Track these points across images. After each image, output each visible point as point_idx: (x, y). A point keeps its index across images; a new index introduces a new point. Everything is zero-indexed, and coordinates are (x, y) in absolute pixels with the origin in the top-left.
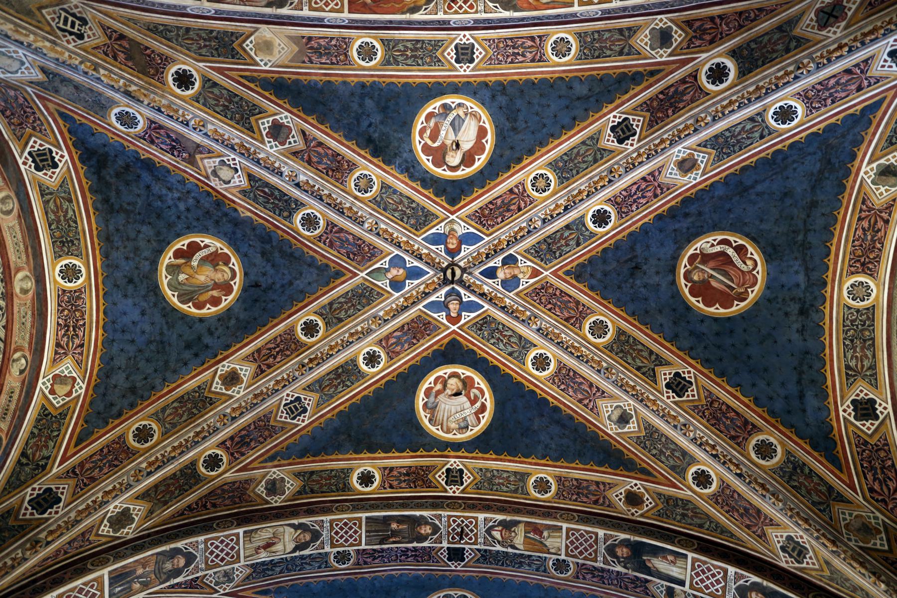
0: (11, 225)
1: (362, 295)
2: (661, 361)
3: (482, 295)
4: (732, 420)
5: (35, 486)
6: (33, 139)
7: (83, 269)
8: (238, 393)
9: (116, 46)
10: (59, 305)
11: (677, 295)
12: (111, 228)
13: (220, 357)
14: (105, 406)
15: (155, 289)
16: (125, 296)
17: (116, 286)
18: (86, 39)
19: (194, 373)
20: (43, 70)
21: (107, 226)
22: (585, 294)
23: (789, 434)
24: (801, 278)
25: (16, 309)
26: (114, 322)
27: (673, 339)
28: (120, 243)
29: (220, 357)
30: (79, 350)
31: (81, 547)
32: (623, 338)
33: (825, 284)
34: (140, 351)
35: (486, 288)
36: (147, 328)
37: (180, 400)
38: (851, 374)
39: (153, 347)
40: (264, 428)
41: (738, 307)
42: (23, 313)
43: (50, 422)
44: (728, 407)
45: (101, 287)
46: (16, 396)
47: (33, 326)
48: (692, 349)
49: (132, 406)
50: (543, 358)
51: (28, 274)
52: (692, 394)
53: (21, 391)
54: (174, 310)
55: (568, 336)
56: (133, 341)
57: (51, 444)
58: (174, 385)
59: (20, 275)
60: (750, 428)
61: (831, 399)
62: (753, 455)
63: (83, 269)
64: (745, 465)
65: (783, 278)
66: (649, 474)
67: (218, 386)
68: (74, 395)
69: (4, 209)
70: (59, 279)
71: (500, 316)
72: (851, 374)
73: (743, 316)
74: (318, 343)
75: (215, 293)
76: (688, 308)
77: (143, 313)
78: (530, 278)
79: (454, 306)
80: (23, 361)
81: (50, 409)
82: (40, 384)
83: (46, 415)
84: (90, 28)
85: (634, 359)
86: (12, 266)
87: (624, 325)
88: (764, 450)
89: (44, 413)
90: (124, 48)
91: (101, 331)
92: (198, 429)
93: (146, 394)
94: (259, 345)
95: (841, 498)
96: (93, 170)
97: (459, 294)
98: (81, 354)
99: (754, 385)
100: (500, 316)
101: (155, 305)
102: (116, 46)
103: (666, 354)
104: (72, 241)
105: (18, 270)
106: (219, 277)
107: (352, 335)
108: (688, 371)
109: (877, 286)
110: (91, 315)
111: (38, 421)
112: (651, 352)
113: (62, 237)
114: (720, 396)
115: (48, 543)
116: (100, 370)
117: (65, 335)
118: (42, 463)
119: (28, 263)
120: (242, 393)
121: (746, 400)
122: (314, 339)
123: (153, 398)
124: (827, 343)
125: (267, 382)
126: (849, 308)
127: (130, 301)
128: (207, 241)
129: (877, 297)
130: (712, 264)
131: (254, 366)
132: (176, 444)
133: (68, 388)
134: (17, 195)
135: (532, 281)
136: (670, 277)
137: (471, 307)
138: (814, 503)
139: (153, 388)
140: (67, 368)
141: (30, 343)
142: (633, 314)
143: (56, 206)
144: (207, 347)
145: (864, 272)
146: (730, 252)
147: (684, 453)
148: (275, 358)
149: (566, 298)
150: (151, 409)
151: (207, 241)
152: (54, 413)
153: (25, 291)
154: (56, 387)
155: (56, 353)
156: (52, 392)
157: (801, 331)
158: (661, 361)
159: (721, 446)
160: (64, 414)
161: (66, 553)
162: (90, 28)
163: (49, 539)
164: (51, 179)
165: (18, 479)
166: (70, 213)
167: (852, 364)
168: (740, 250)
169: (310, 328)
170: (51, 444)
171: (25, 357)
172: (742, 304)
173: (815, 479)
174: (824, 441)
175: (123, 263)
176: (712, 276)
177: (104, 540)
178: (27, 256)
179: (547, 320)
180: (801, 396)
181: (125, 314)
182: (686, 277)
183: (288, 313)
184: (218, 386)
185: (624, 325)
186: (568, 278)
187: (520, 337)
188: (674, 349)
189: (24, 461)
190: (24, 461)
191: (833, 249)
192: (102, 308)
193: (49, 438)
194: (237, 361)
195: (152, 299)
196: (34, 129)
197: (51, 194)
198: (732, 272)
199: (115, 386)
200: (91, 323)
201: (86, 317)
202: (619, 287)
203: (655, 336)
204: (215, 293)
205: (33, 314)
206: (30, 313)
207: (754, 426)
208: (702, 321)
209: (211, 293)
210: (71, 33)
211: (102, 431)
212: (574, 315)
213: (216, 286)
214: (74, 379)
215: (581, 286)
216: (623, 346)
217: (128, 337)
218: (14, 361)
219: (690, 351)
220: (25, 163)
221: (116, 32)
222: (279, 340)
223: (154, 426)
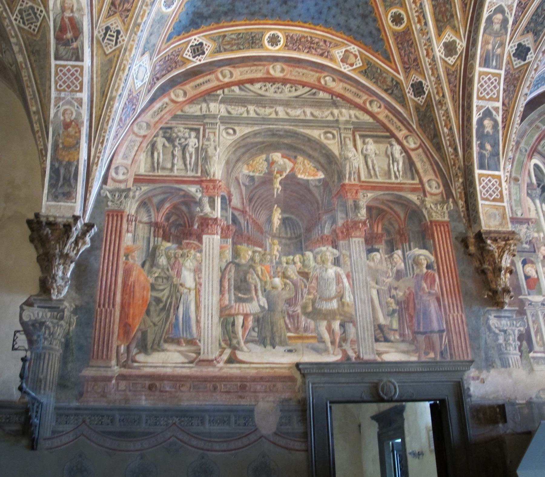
0: (239, 73)
5: (407, 91)
6: (184, 55)
7: (272, 32)
9: (120, 9)
10: (295, 50)
12: (245, 11)
16: (295, 7)
17: (287, 12)
18: (119, 28)
20: (143, 54)
21: (244, 14)
25: (293, 78)
28: (257, 7)
30: (328, 44)
31: (456, 77)
42: (296, 74)
46: (348, 87)
47: (306, 69)
49: (375, 20)
51: (271, 66)
53: (346, 83)
56: (329, 8)
57: (384, 75)
59: (272, 72)
63: (272, 32)
68: (357, 53)
69: (229, 76)
70: (277, 48)
80: (327, 78)
81: (363, 69)
82: (346, 71)
83: (366, 72)
84: (112, 25)
86: (265, 76)
89: (365, 73)
90: (120, 3)
93: (369, 8)
96: (204, 21)
102: (120, 9)
104: (252, 37)
105: (268, 72)
110: (305, 32)
111: (367, 77)
113: (249, 43)
115: (444, 96)
116: (344, 33)
117: (315, 50)
119: (264, 65)
123: (374, 4)
134: (220, 67)
140: (338, 53)
141: (317, 72)
143: (228, 44)
152: (366, 67)
153: (283, 70)
155: (327, 57)
156: (352, 65)
160: (368, 62)
161: (455, 86)
162: (112, 25)
163: (441, 95)
164: (209, 46)
165: (400, 98)
166: (233, 36)
170: (384, 75)
171: (325, 77)
175: (271, 6)
177: (459, 62)
178: (260, 65)
189: (390, 91)
190: (390, 91)
193: (381, 74)
196: (178, 55)
197: (220, 47)
199: (358, 27)
201: (306, 35)
205: (298, 67)
206: (297, 69)
210: (117, 38)
211: (386, 44)
214: (346, 51)
217: (325, 10)
218: (326, 84)
220: (200, 60)
221: (110, 8)
223: (394, 10)
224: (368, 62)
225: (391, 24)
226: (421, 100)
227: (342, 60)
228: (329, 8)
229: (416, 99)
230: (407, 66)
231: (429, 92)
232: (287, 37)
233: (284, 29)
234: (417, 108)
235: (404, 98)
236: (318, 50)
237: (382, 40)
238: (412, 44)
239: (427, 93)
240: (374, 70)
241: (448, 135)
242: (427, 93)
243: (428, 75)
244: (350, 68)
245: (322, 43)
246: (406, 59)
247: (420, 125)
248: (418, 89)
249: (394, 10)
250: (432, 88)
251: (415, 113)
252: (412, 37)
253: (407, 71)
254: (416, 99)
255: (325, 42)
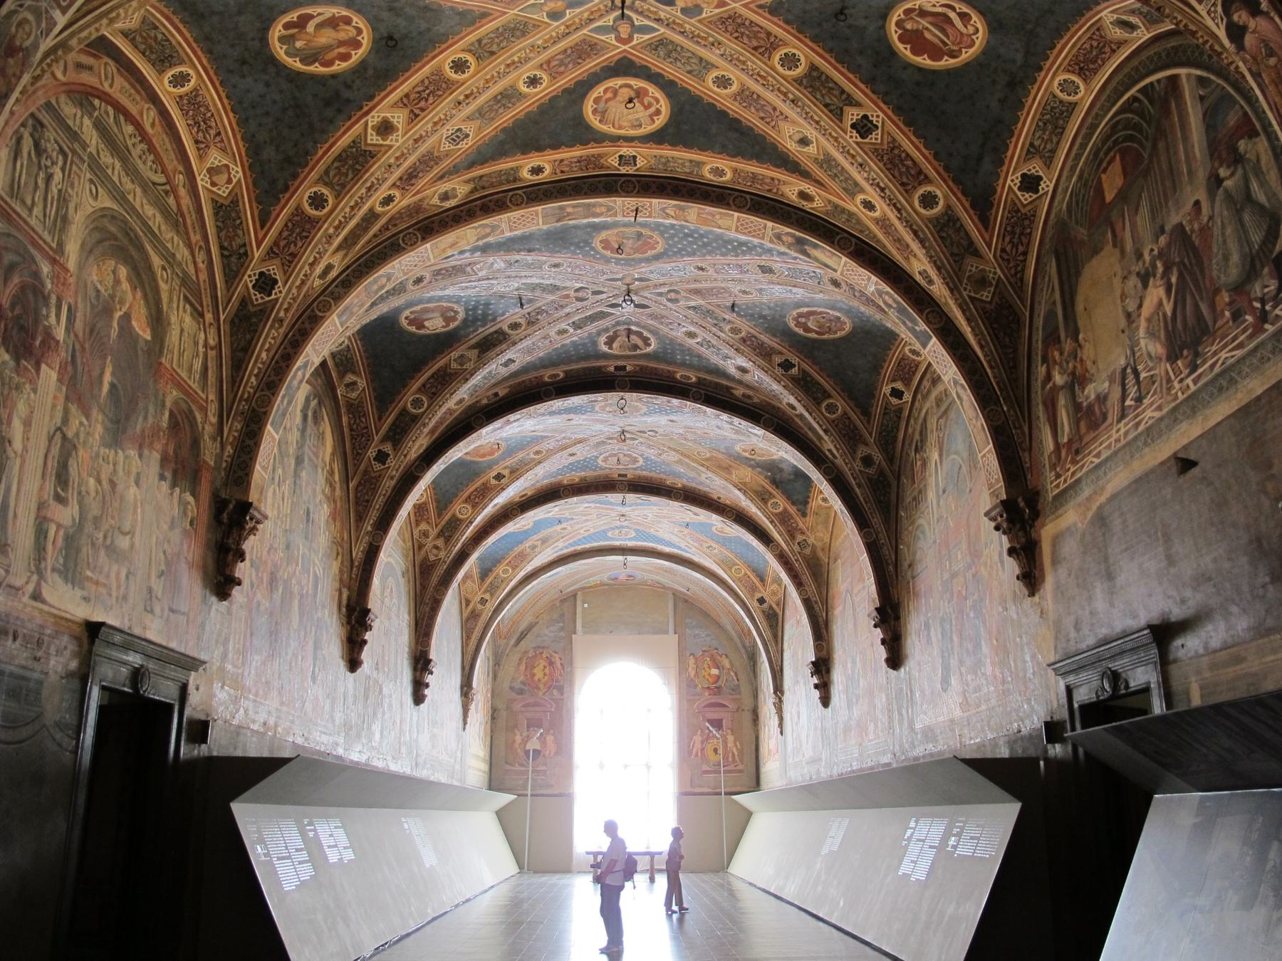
1: (514, 30)
2: (851, 101)
3: (658, 20)
4: (908, 168)
5: (249, 272)
7: (191, 72)
8: (397, 141)
11: (883, 39)
13: (366, 109)
14: (271, 180)
15: (273, 60)
16: (244, 77)
17: (231, 72)
19: (343, 129)
22: (779, 26)
23: (955, 189)
24: (1019, 57)
26: (240, 103)
27: (870, 81)
29: (366, 109)
30: (218, 139)
32: (815, 74)
33: (1040, 69)
34: (278, 120)
35: (662, 15)
36: (277, 97)
37: (339, 158)
38: (1032, 151)
39: (290, 113)
40: (429, 160)
41: (947, 62)
43: (227, 212)
44: (908, 155)
45: (215, 78)
48: (886, 94)
50: (726, 78)
52: (876, 137)
54: (299, 73)
55: (755, 63)
56: (267, 114)
58: (327, 145)
60: (921, 177)
61: (1005, 168)
62: (916, 203)
63: (191, 72)
64: (906, 211)
65: (1002, 51)
66: (822, 185)
67: (372, 138)
68: (235, 181)
70: (172, 89)
71: (678, 39)
72: (1032, 151)
73: (949, 72)
74: (471, 79)
75: (342, 50)
76: (893, 53)
77: (267, 85)
78: (717, 7)
79: (624, 30)
82: (200, 183)
85: (823, 96)
87: (818, 61)
88: (929, 201)
89: (218, 207)
91: (231, 115)
92: (368, 184)
94: (406, 91)
95: (976, 253)
97: (630, 19)
98: (222, 141)
99: (938, 140)
100: (678, 39)
101: (278, 74)
103: (858, 95)
106: (342, 36)
107: (508, 66)
108: (877, 115)
109: (1086, 90)
110: (215, 105)
111: (216, 214)
112: (843, 92)
114: (903, 144)
118: (242, 251)
120: (401, 141)
121: (926, 152)
122: (466, 75)
124: (1022, 118)
125: (423, 126)
126: (1055, 96)
127: (249, 80)
128: (320, 10)
129: (1082, 98)
130: (930, 19)
131: (406, 111)
132: (352, 203)
133: (226, 176)
135: (717, 11)
136: (880, 23)
137: (643, 30)
138: (952, 254)
139: (307, 153)
142: (830, 51)
144: (348, 101)
145: (1079, 75)
146: (952, 15)
147: (856, 184)
148: (427, 100)
149: (756, 29)
150: (314, 175)
151: (320, 10)
152: (226, 203)
154: (215, 179)
155: (199, 149)
156: (214, 184)
157: (1002, 101)
158: (851, 101)
159: (890, 190)
160: (235, 201)
166: (160, 36)
167: (1037, 143)
168: (964, 17)
169: (459, 66)
170: (240, 232)
172: (952, 61)
173: (962, 234)
174: (982, 204)
176: (927, 29)
179: (732, 46)
180: (980, 159)
181: (248, 91)
182: (899, 24)
183: (431, 55)
184: (372, 138)
185: (818, 61)
186: (760, 11)
187: (701, 59)
188: (868, 91)
189: (226, 253)
191: (1059, 46)
192: (223, 95)
193: (236, 227)
194: (387, 108)
195: (272, 70)
198: (950, 31)
200: (218, 110)
201: (211, 108)
202: (819, 25)
203: (851, 76)
204: (342, 50)
207: (926, 177)
208: (905, 68)
209: (337, 51)
212: (765, 46)
213: (341, 43)
214: (227, 166)
215: (775, 19)
216: (814, 81)
219: (885, 97)
222: (426, 82)
223: (325, 191)
224: (235, 201)
225: (306, 197)
226: (258, 298)
227: (210, 171)
228: (267, 114)
229: (252, 291)
230: (275, 249)
231: (277, 300)
232: (195, 89)
233: (204, 81)
234: (244, 302)
235: (236, 276)
236: (201, 134)
237: (279, 200)
238: (306, 238)
239: (273, 297)
240: (233, 215)
241: (263, 363)
242: (273, 297)
243: (293, 283)
244: (208, 186)
245: (213, 132)
246: (282, 243)
247: (232, 322)
248: (266, 284)
249: (325, 191)
250: (284, 299)
251: (237, 304)
252: (313, 232)
253: (271, 254)
254: (252, 291)
255: (219, 134)
